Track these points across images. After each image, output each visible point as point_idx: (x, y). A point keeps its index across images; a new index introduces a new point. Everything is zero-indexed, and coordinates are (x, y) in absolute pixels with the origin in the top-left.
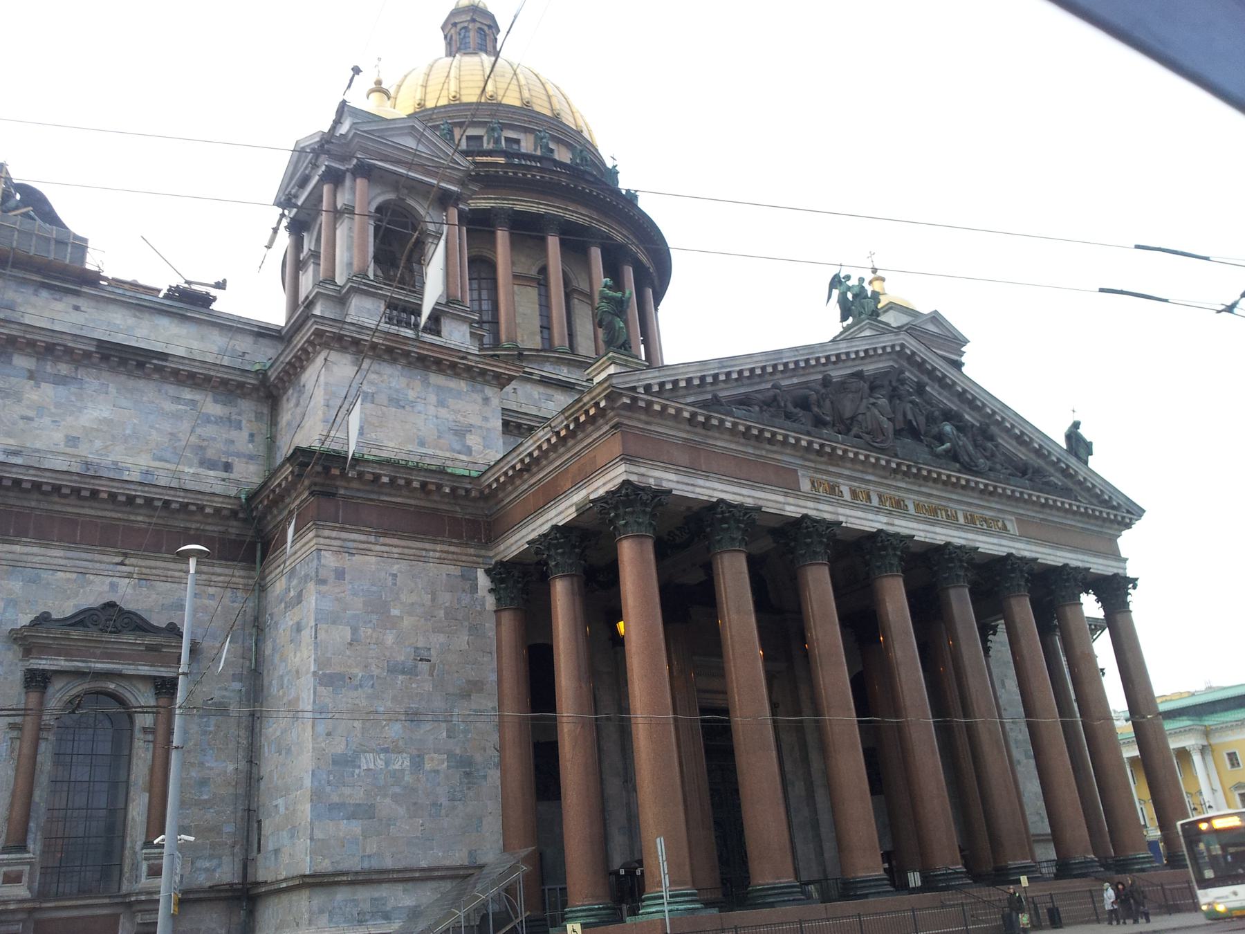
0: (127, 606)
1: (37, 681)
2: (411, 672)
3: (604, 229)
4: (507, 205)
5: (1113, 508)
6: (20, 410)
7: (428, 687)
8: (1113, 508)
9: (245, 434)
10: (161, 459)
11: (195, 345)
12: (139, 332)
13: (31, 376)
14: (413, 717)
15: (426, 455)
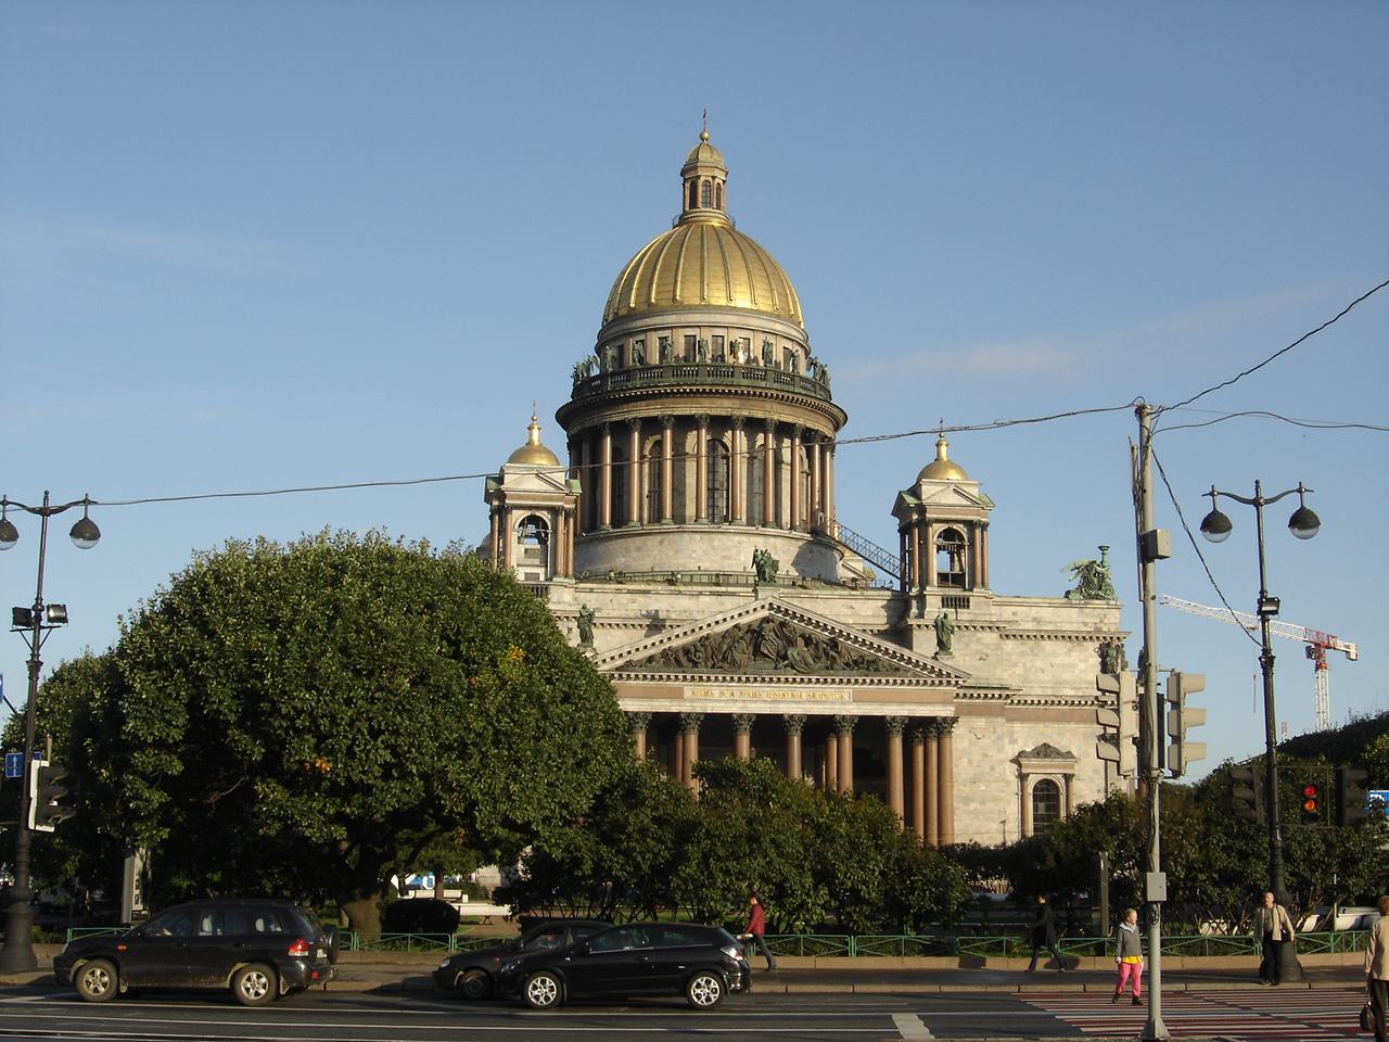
3: (746, 413)
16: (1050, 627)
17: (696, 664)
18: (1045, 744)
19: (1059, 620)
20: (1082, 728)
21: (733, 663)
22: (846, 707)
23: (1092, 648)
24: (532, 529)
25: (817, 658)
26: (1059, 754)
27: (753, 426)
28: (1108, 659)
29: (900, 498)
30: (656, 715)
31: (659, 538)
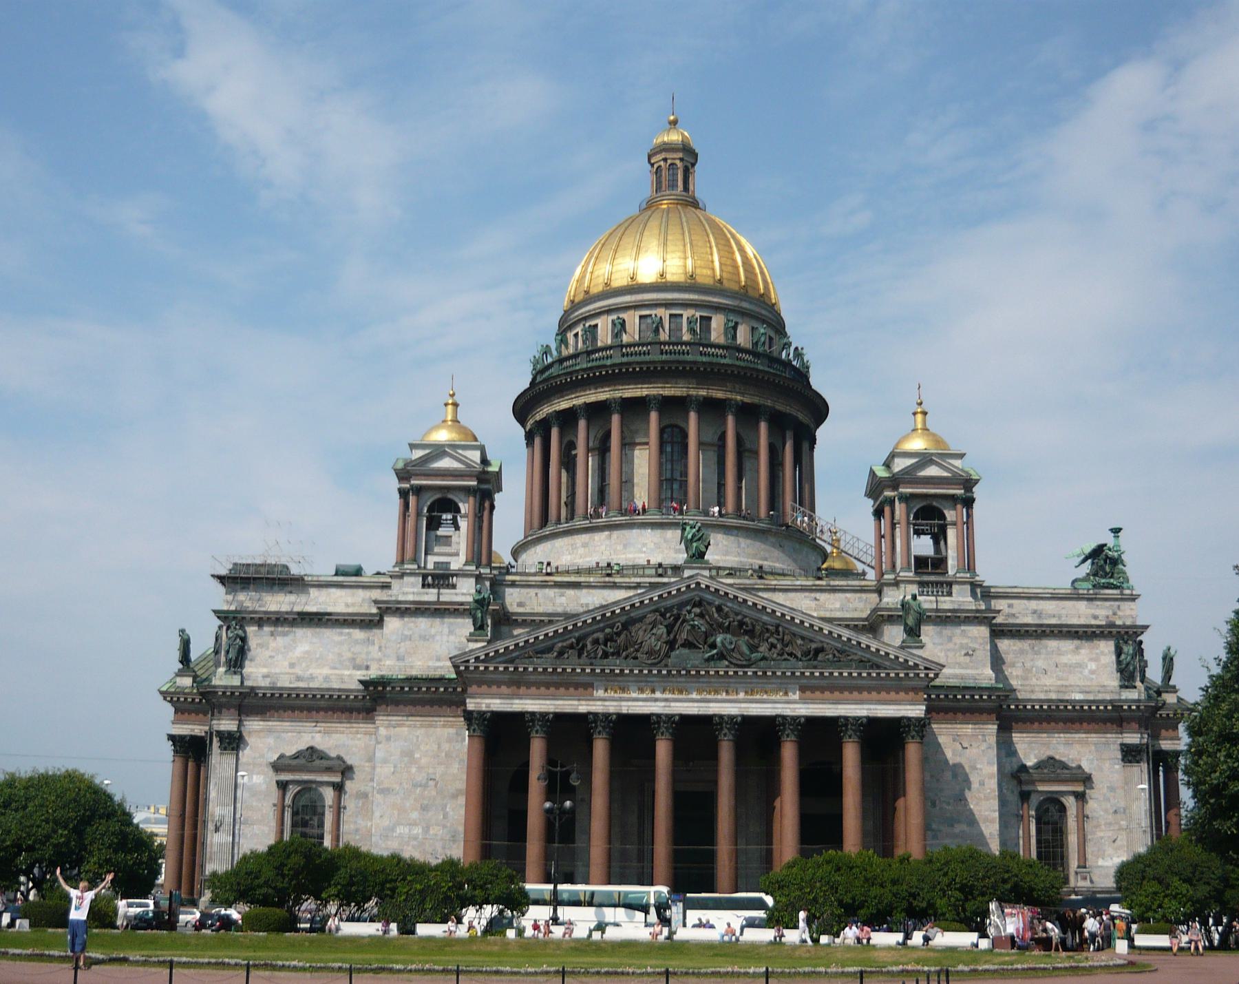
0: (320, 747)
1: (283, 786)
2: (425, 786)
3: (703, 393)
4: (618, 394)
5: (910, 668)
6: (268, 653)
7: (434, 793)
8: (910, 668)
9: (377, 647)
10: (335, 668)
11: (350, 600)
12: (321, 599)
13: (272, 634)
14: (424, 808)
15: (436, 668)
16: (1053, 621)
17: (606, 655)
18: (1052, 758)
19: (1064, 612)
20: (1094, 738)
21: (650, 653)
22: (792, 706)
23: (1106, 648)
24: (447, 516)
25: (753, 648)
26: (1064, 766)
27: (712, 409)
28: (1123, 657)
29: (872, 473)
30: (560, 717)
31: (607, 533)
